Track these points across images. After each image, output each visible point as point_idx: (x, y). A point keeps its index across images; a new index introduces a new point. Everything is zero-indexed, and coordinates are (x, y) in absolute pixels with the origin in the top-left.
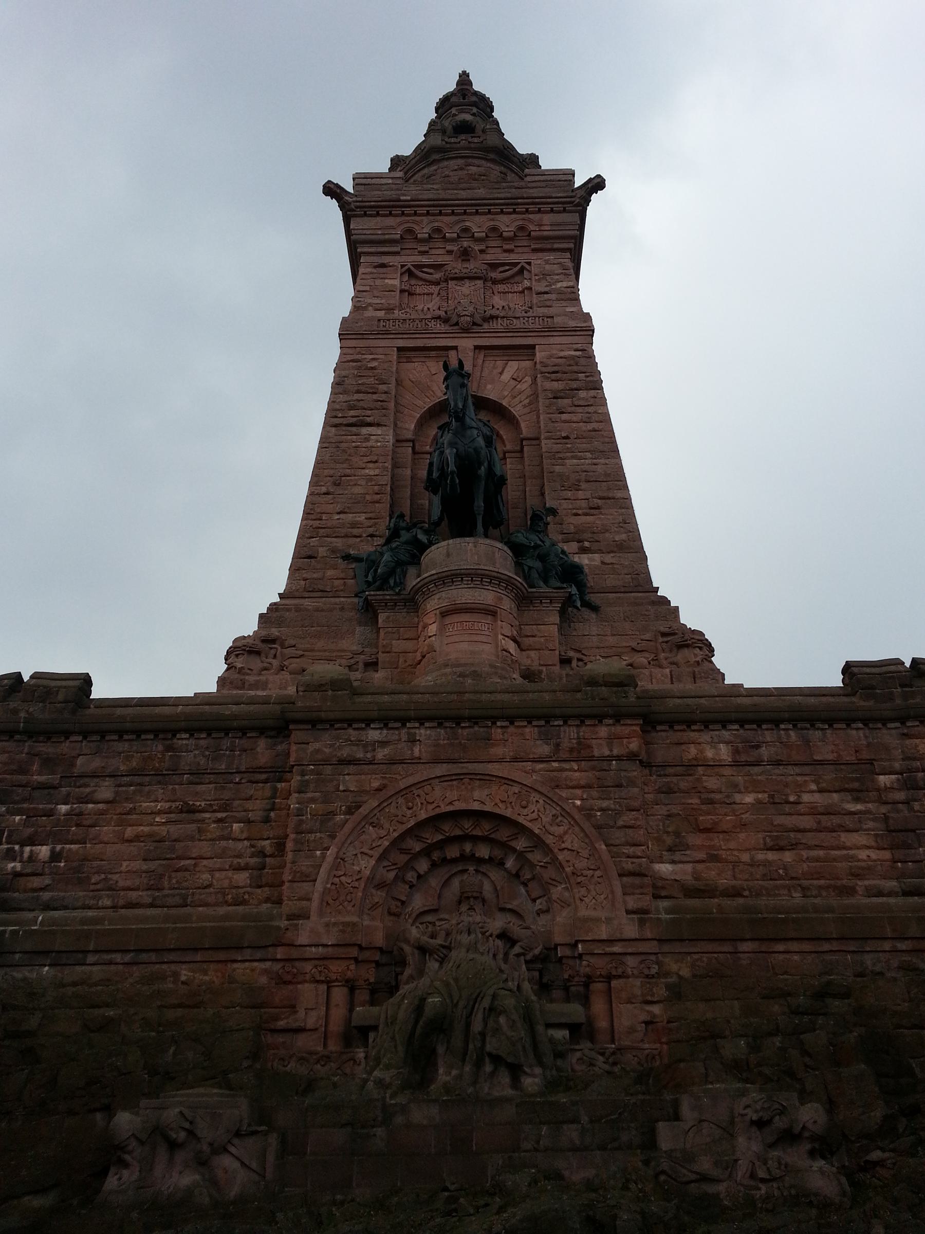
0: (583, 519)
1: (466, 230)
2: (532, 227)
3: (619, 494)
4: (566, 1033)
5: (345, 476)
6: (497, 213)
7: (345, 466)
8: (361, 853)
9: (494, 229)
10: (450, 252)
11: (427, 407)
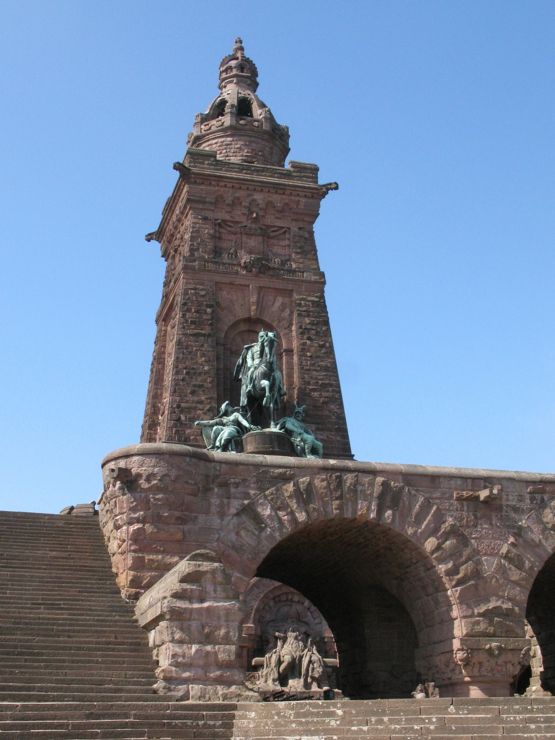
1: (254, 200)
2: (294, 206)
4: (331, 669)
6: (272, 193)
8: (253, 599)
9: (271, 202)
10: (244, 214)
11: (232, 322)
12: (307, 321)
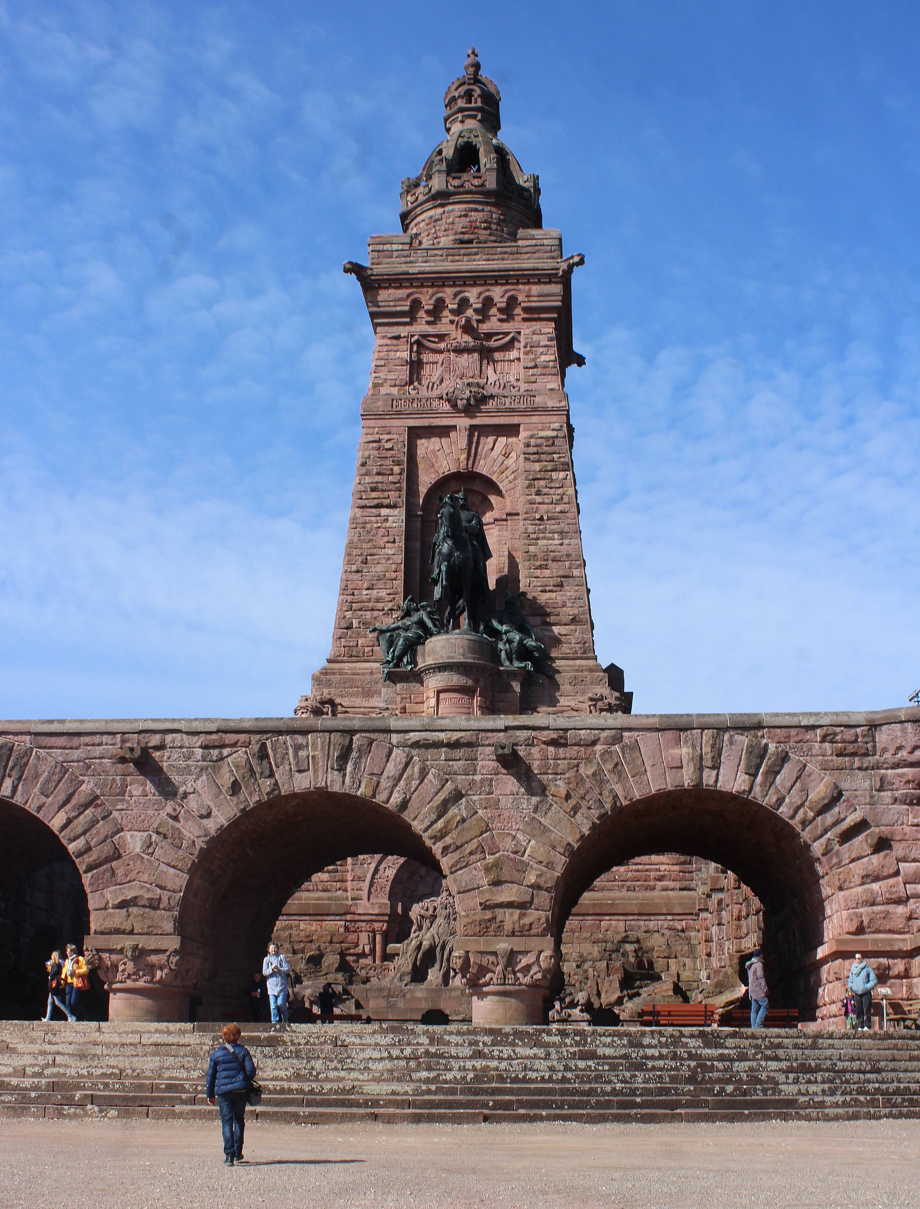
0: (548, 595)
3: (576, 572)
7: (369, 545)
12: (537, 466)
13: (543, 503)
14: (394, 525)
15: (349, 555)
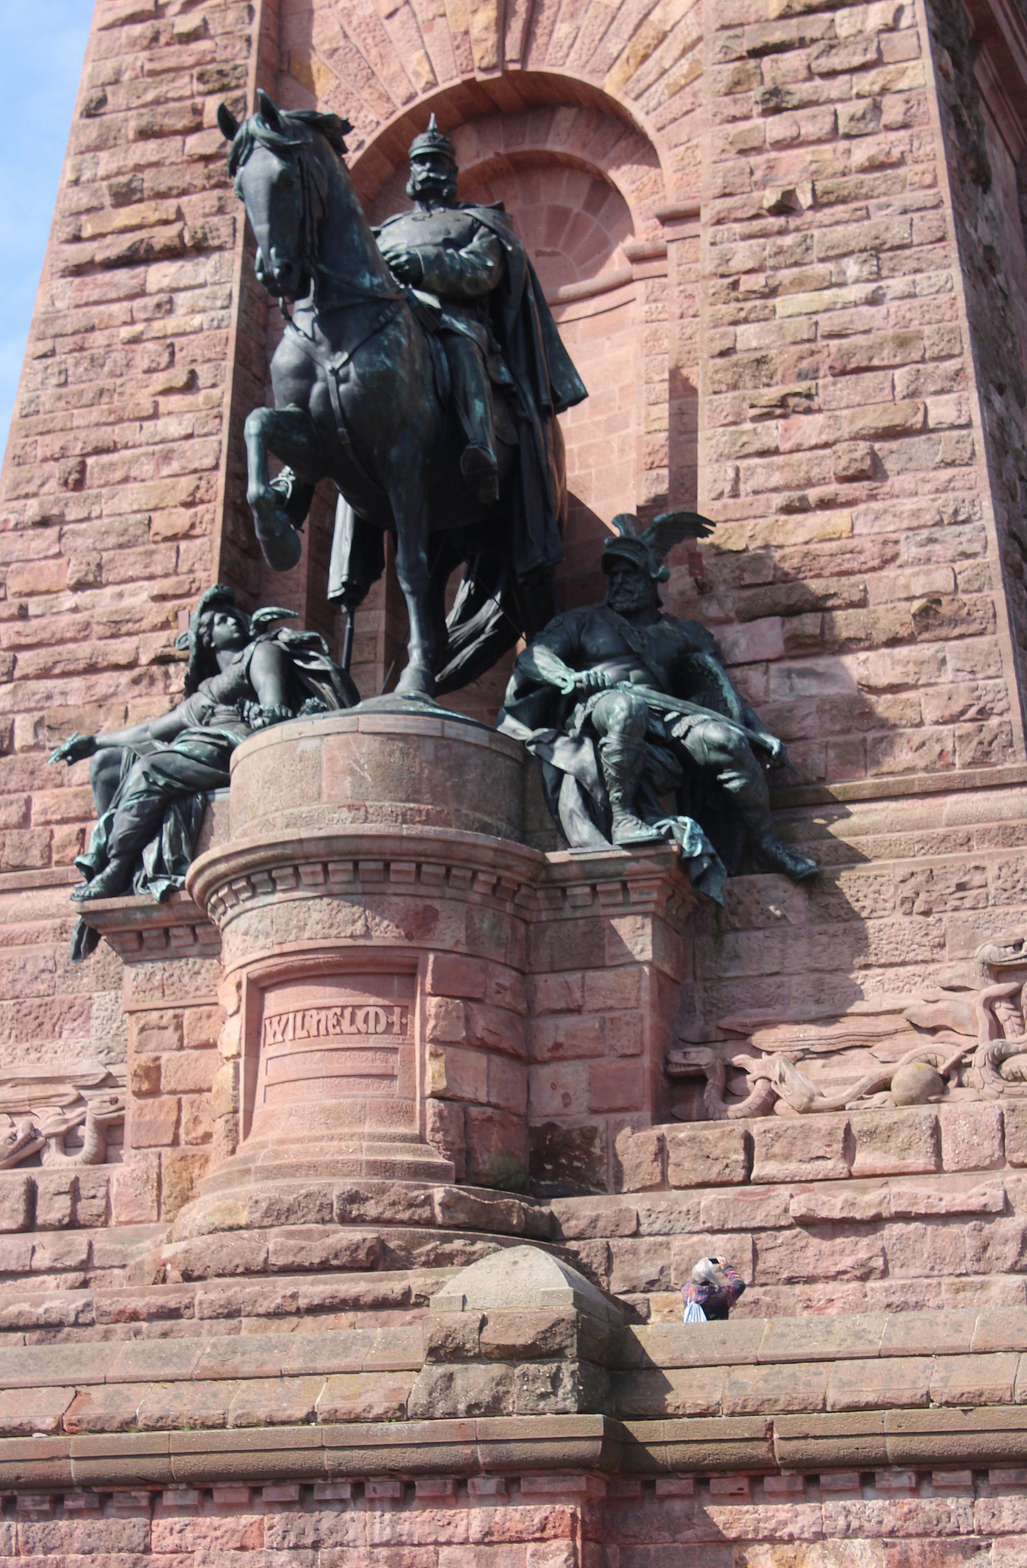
0: (816, 521)
5: (98, 451)
7: (95, 415)
13: (794, 143)
14: (197, 320)
15: (19, 461)
